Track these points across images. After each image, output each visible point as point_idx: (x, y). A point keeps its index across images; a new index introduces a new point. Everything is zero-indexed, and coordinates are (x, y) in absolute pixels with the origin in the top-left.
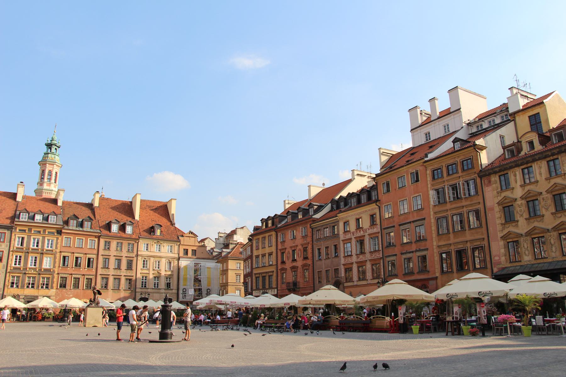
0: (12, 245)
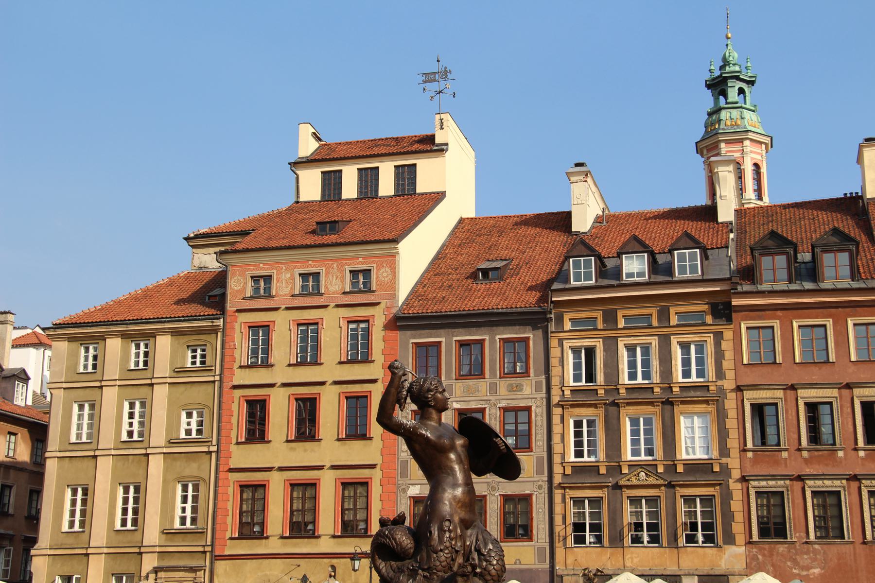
0: (555, 382)
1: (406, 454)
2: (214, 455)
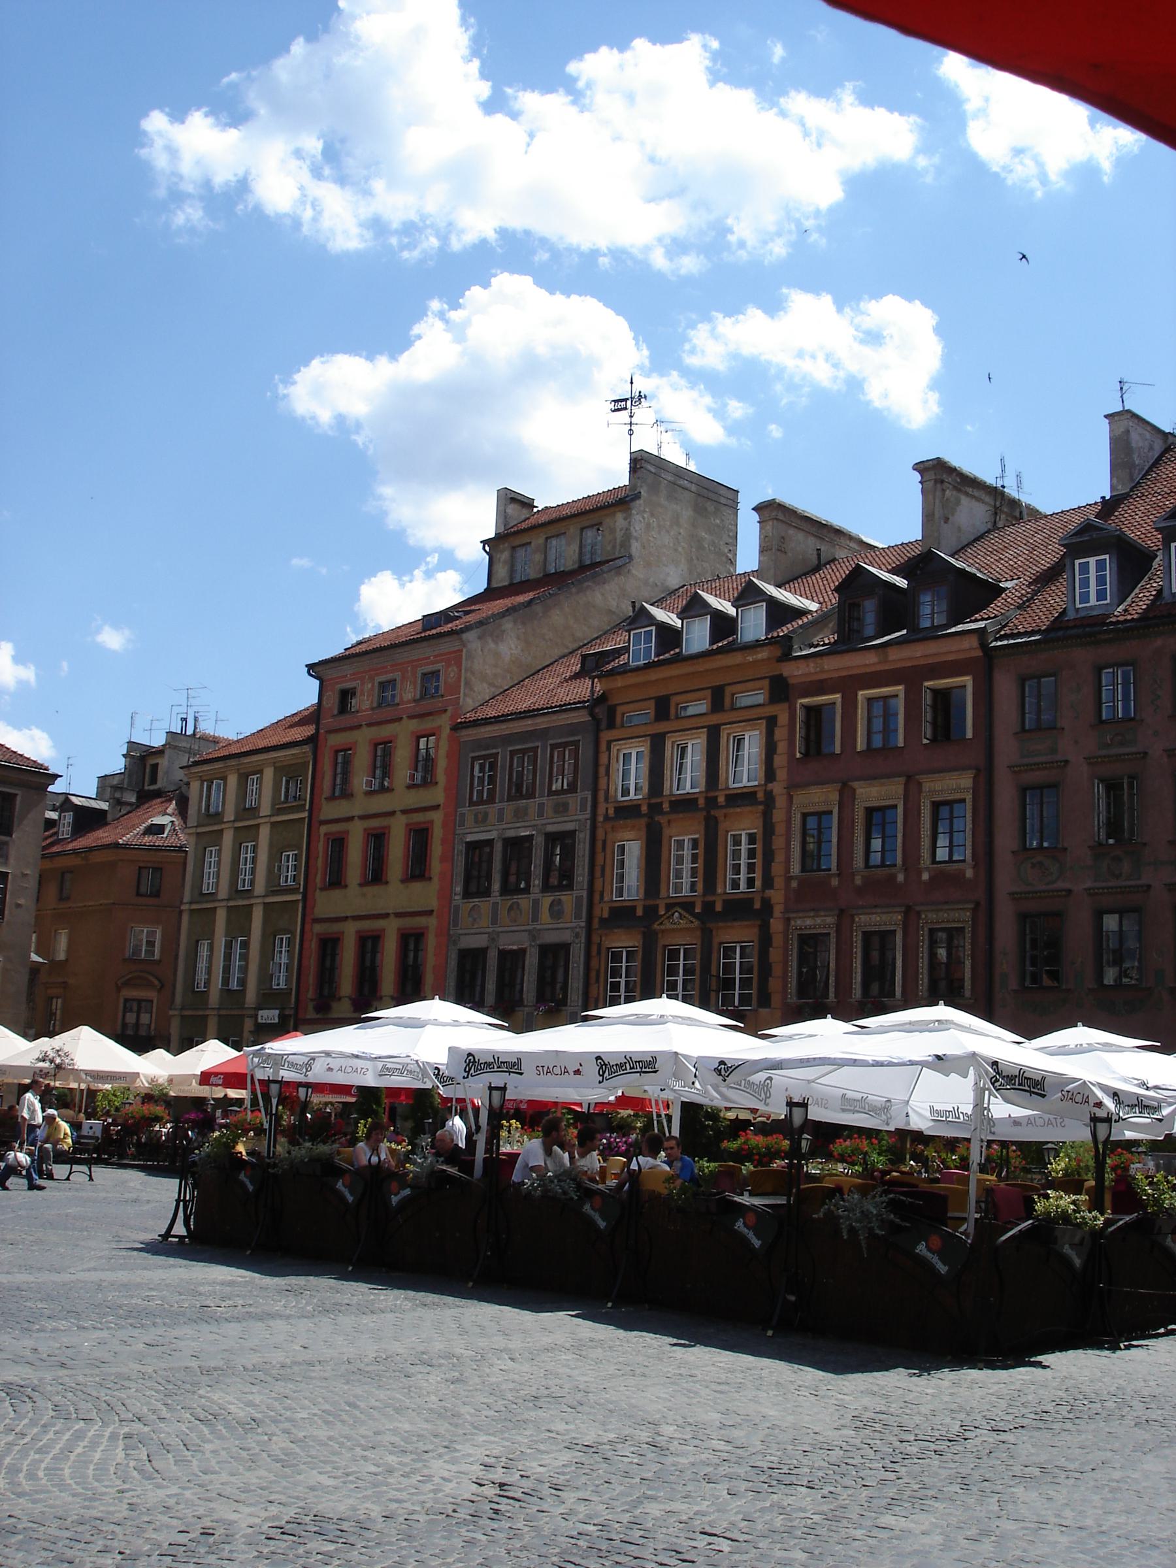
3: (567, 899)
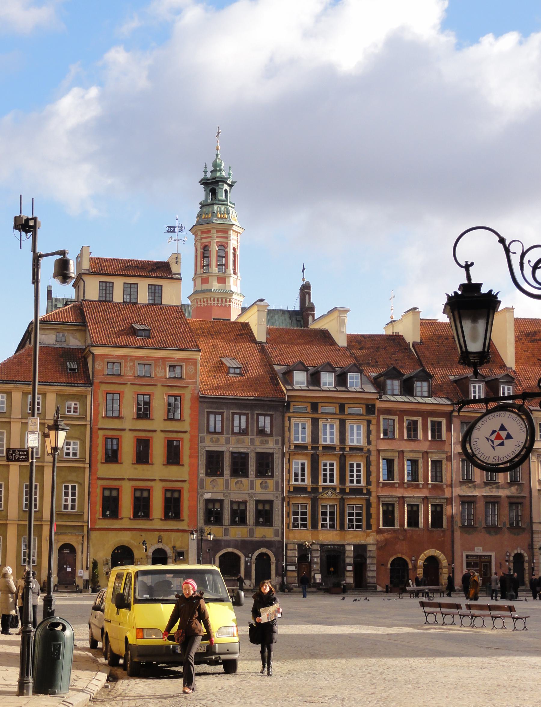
0: (286, 439)
1: (202, 475)
2: (87, 471)
3: (271, 482)
